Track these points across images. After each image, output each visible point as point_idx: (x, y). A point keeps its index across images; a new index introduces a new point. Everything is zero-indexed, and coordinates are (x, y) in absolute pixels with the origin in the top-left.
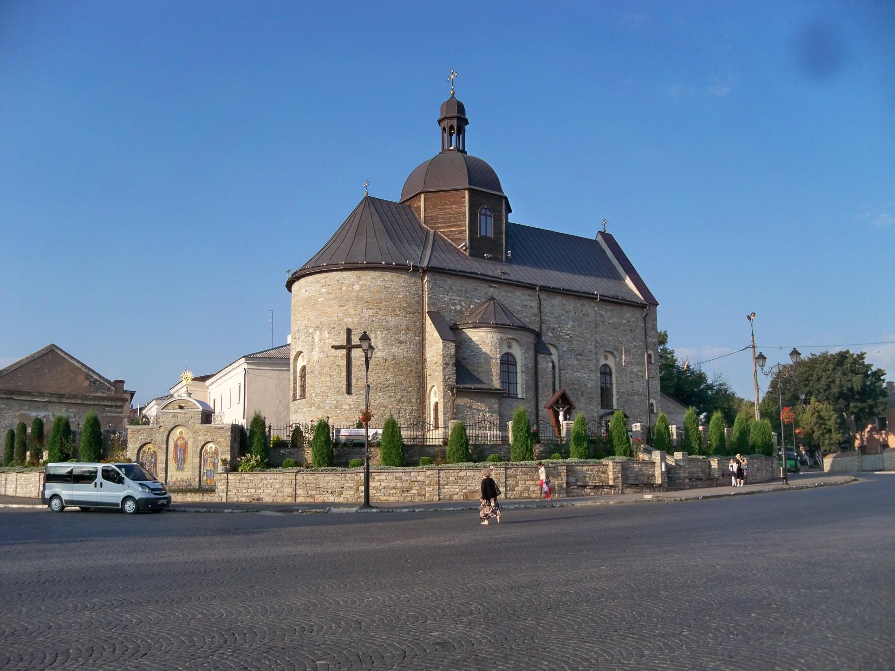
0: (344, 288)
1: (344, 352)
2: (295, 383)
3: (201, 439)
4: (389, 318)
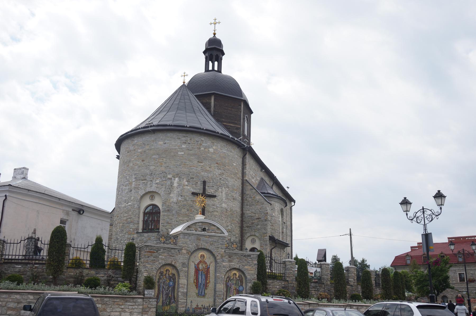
0: (202, 149)
4: (229, 179)
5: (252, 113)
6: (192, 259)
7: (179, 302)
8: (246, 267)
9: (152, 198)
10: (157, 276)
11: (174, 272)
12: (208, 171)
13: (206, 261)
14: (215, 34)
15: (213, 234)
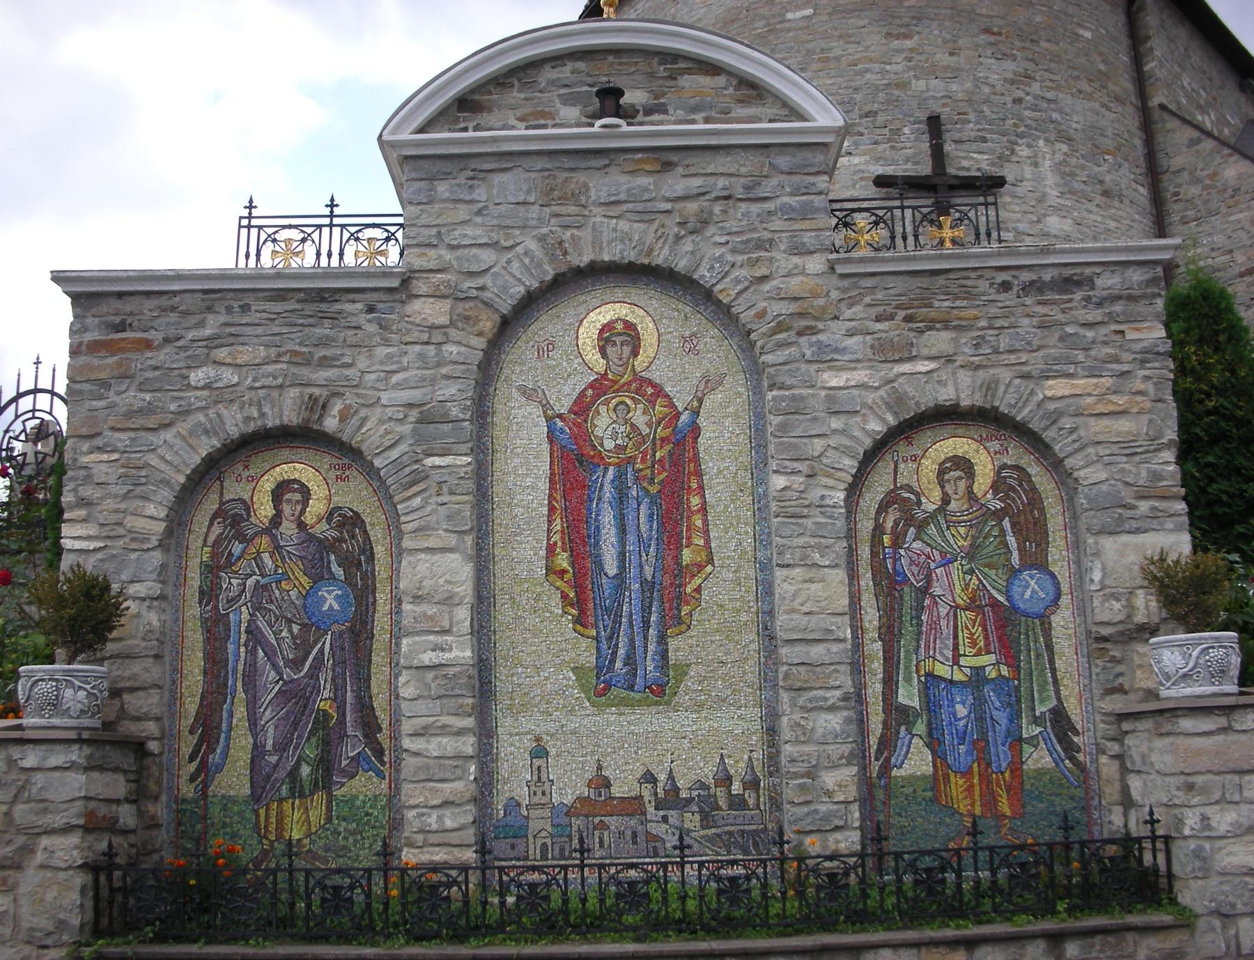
3: (854, 383)
4: (1066, 100)
6: (523, 363)
7: (409, 763)
8: (1056, 387)
10: (195, 542)
11: (355, 495)
12: (946, 68)
13: (655, 376)
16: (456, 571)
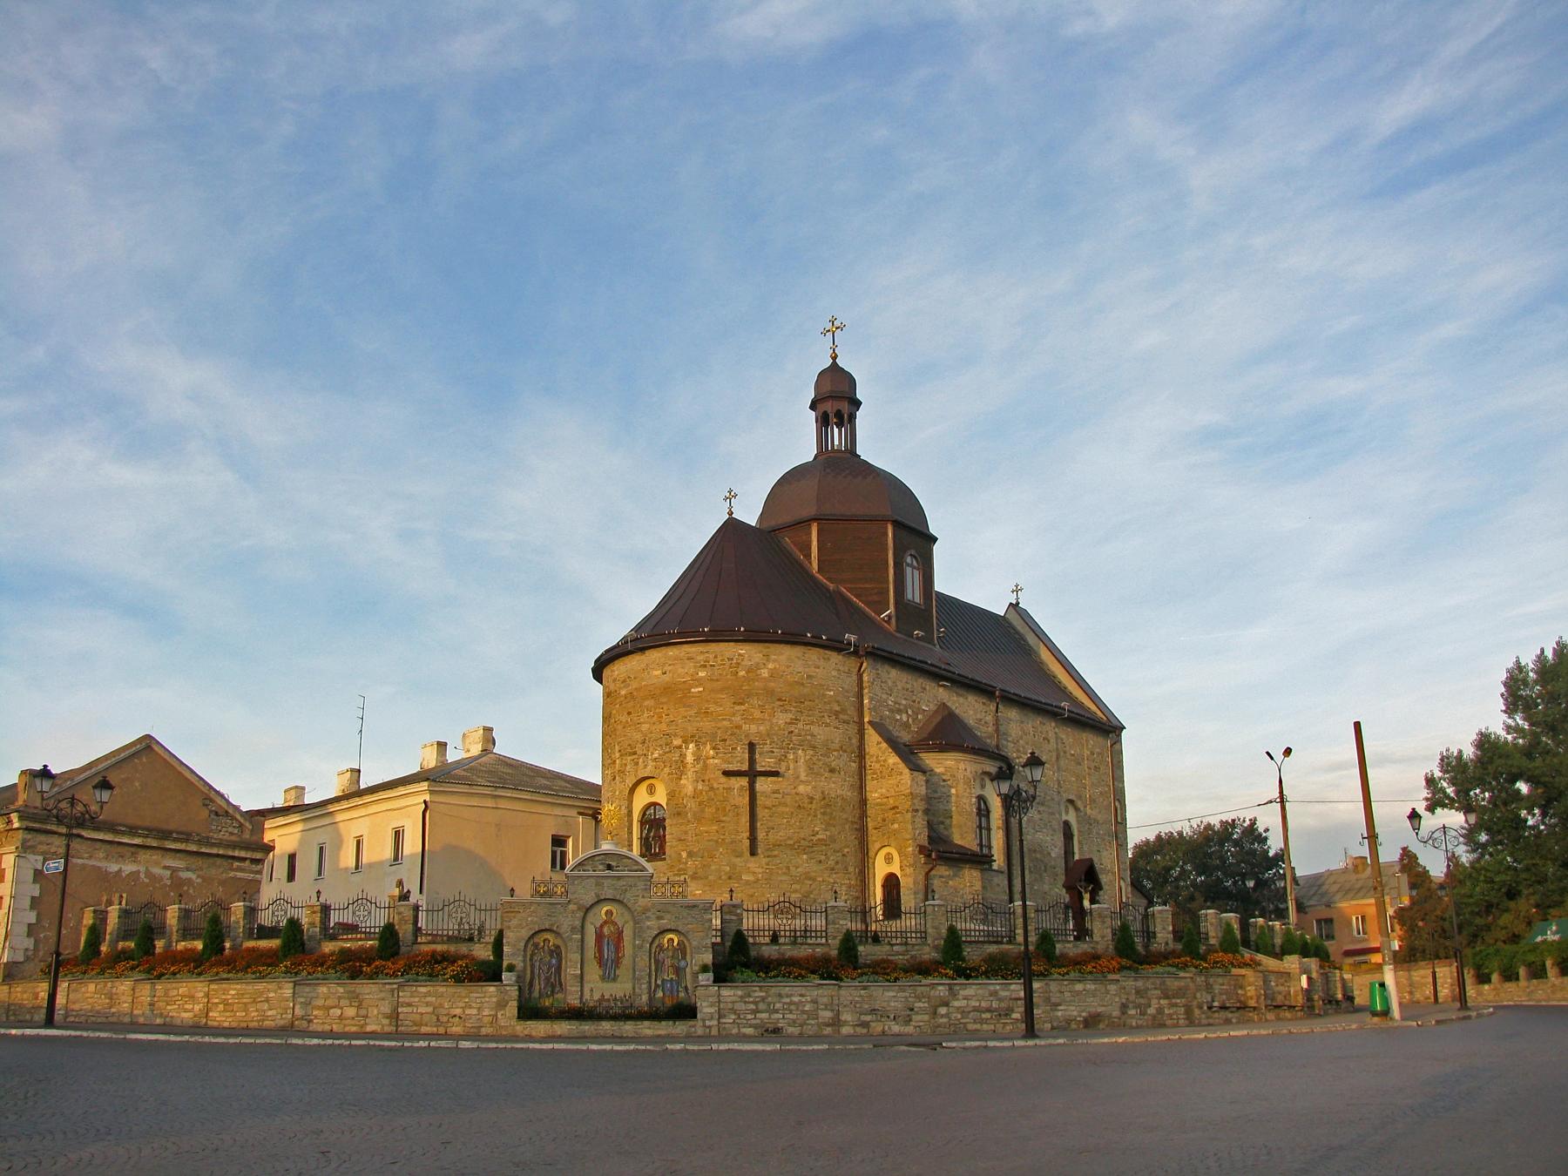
1: (744, 781)
2: (630, 833)
3: (653, 925)
4: (815, 729)
5: (935, 540)
6: (591, 914)
9: (651, 790)
14: (834, 358)
15: (626, 873)
16: (577, 957)
